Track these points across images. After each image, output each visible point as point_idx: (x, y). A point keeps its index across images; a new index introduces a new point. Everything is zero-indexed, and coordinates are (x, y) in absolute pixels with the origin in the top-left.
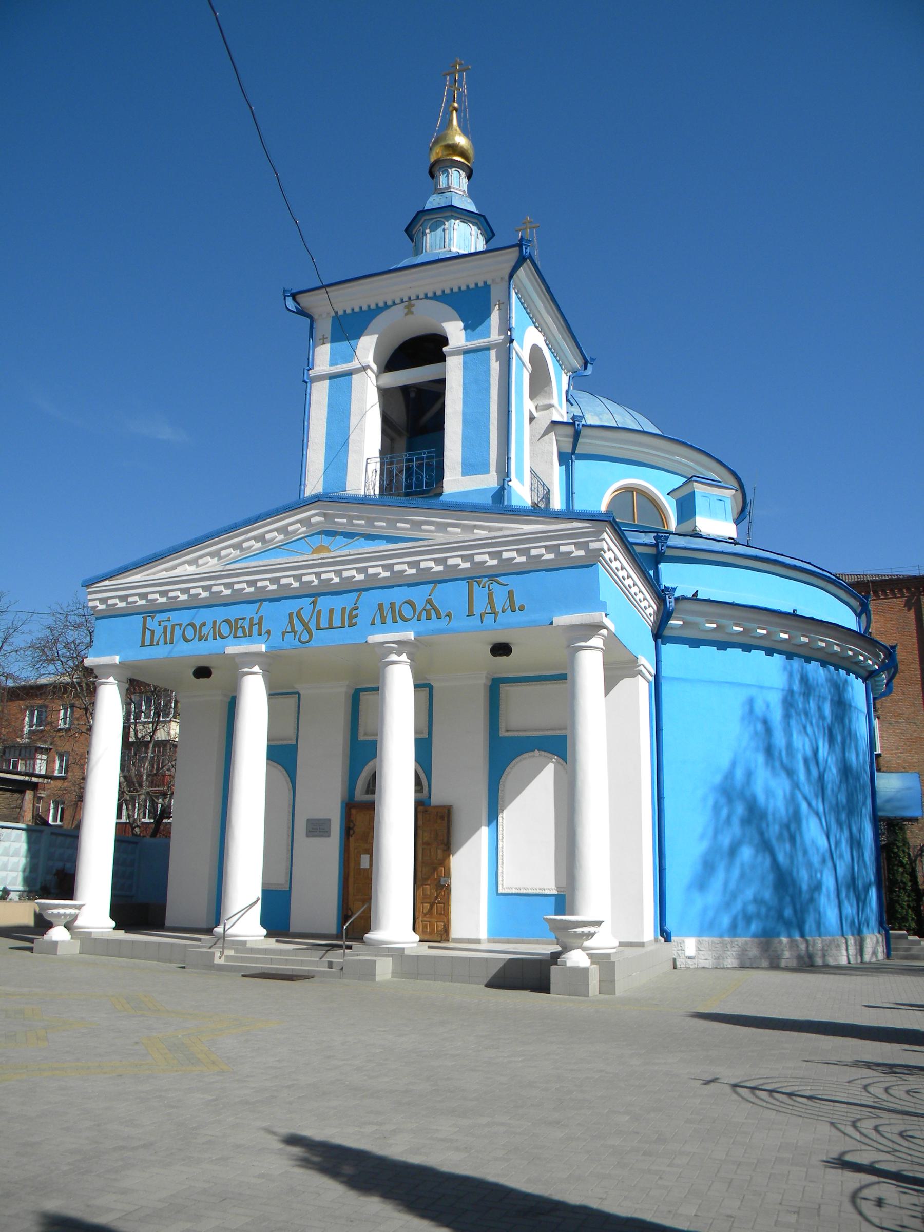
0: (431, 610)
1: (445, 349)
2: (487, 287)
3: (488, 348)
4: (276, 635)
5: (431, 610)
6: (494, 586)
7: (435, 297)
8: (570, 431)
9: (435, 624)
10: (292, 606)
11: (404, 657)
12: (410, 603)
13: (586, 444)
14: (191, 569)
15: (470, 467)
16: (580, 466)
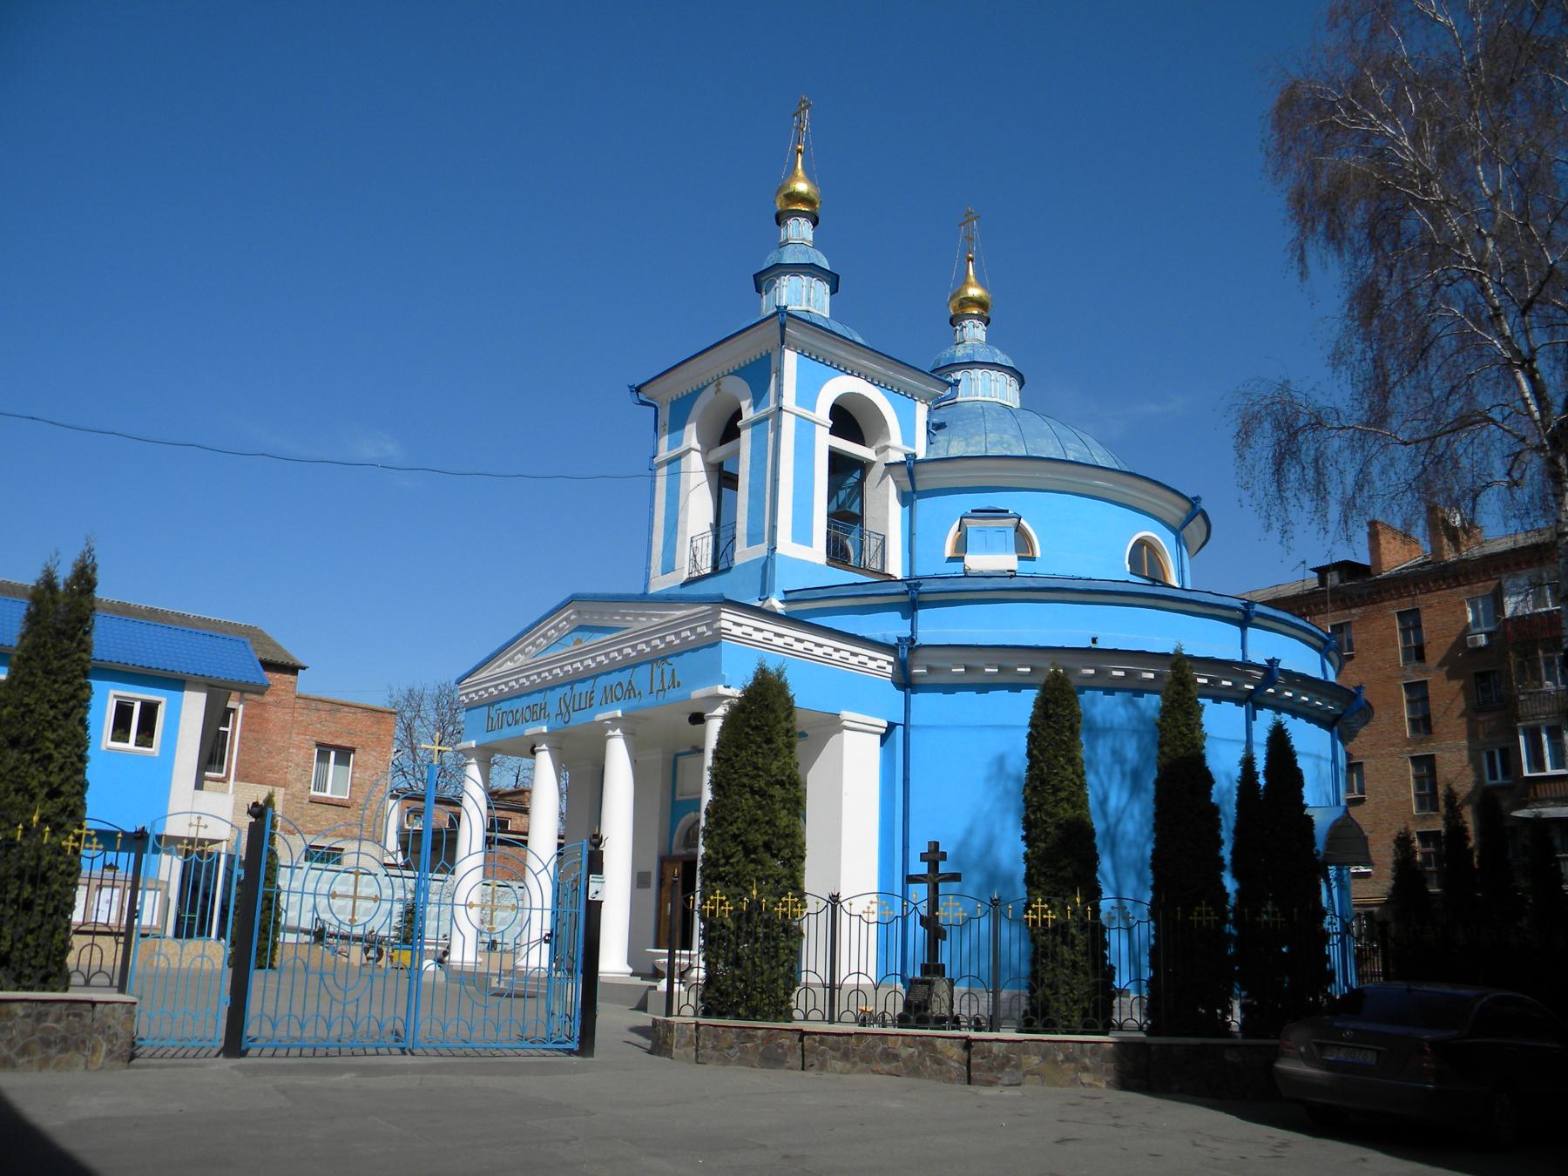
0: (631, 691)
1: (739, 424)
2: (769, 355)
3: (767, 419)
4: (553, 716)
5: (631, 691)
6: (665, 666)
7: (735, 373)
8: (904, 470)
9: (634, 702)
10: (560, 692)
11: (618, 732)
12: (620, 684)
13: (925, 480)
14: (510, 665)
15: (753, 539)
16: (922, 504)
